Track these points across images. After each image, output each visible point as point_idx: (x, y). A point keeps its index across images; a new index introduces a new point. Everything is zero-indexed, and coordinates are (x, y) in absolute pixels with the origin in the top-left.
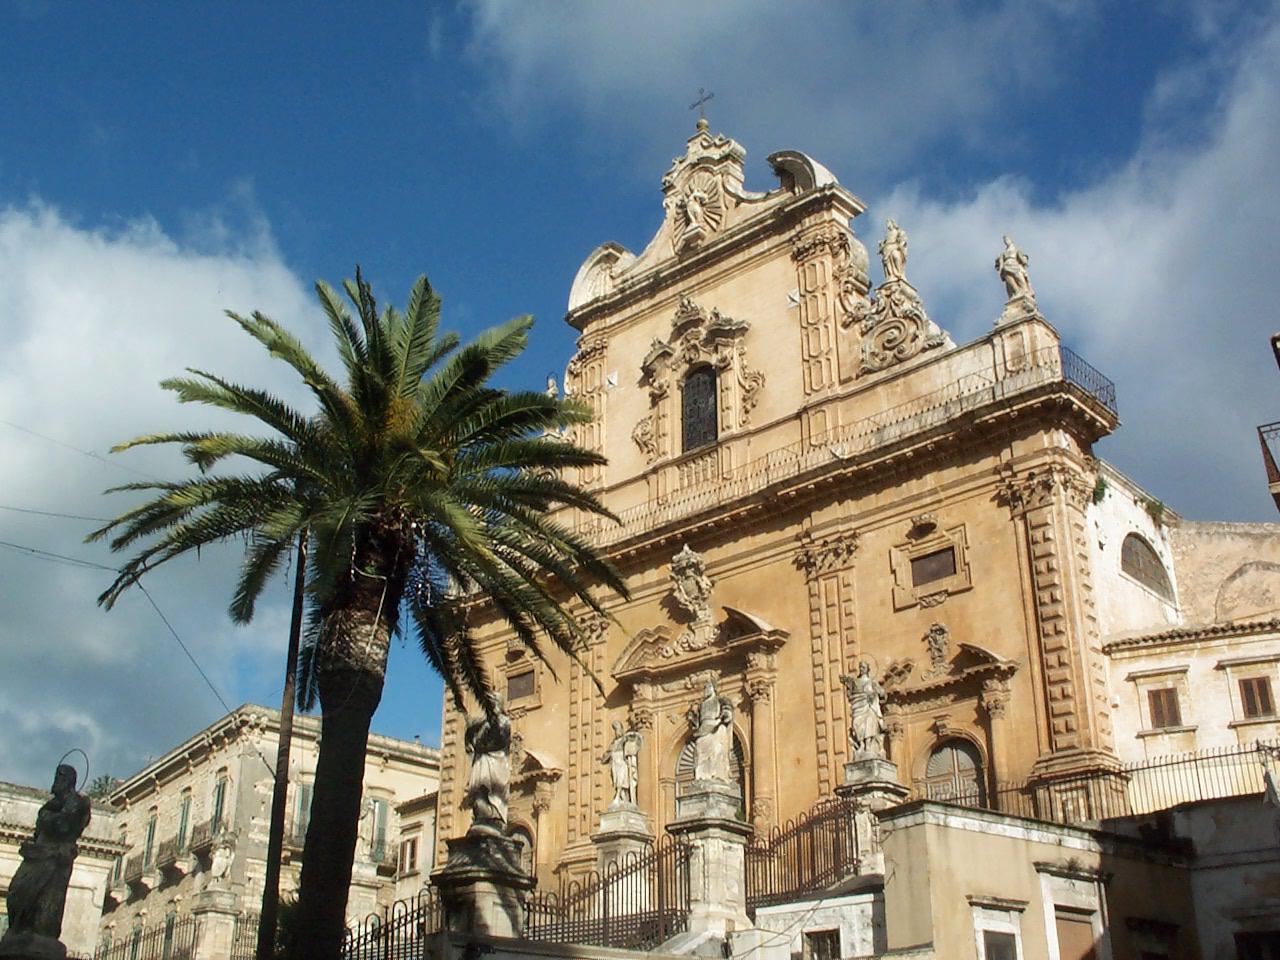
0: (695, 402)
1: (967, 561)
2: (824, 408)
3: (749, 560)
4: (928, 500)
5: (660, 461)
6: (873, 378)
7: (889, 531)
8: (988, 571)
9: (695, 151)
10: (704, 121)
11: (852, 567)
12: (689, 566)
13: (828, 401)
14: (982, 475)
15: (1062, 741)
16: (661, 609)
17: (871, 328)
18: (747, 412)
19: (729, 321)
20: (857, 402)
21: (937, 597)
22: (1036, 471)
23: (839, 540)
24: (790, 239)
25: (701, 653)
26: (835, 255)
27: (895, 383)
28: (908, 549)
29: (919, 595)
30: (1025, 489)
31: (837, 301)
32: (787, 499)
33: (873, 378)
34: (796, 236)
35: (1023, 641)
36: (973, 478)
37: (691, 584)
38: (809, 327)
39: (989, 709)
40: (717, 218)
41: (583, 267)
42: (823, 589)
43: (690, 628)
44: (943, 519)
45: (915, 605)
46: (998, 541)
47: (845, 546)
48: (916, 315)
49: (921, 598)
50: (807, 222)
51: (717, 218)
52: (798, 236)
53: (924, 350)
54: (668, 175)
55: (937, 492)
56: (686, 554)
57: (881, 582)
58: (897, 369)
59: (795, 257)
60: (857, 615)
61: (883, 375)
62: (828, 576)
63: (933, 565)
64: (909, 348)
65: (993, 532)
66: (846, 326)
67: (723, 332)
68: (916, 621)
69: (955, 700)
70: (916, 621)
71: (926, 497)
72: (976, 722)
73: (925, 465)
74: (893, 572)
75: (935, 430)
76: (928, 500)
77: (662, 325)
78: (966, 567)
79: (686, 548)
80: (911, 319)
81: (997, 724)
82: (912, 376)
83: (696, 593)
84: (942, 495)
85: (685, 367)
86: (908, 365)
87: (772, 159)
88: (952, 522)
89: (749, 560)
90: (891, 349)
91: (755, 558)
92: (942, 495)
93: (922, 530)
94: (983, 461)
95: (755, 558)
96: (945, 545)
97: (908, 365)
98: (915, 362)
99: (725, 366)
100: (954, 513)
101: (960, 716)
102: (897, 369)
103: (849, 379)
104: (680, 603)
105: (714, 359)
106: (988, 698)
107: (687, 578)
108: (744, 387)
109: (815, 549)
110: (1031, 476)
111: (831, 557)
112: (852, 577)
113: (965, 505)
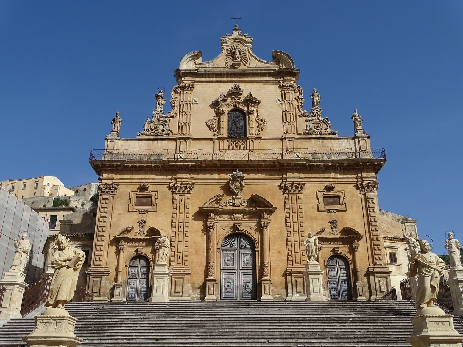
0: (234, 121)
1: (345, 202)
2: (293, 140)
3: (260, 181)
4: (332, 180)
5: (220, 136)
6: (310, 136)
7: (316, 186)
8: (352, 207)
9: (236, 34)
10: (237, 25)
11: (302, 194)
12: (239, 177)
13: (295, 138)
14: (351, 178)
15: (378, 263)
16: (221, 190)
17: (310, 121)
18: (259, 131)
19: (255, 99)
20: (304, 142)
21: (334, 211)
22: (371, 182)
23: (299, 184)
24: (279, 81)
25: (237, 208)
26: (295, 92)
27: (319, 140)
28: (323, 193)
29: (327, 209)
30: (366, 186)
31: (297, 107)
32: (283, 165)
33: (310, 136)
34: (283, 80)
35: (363, 230)
36: (348, 178)
37: (238, 183)
38: (285, 111)
40: (246, 61)
41: (186, 55)
42: (290, 198)
43: (233, 198)
44: (338, 187)
45: (325, 211)
46: (355, 199)
47: (300, 187)
48: (327, 122)
49: (328, 210)
50: (286, 78)
51: (246, 61)
52: (283, 81)
53: (329, 134)
54: (224, 38)
55: (335, 179)
56: (238, 173)
57: (312, 201)
58: (318, 136)
59: (280, 87)
60: (303, 209)
61: (314, 136)
62: (292, 194)
63: (331, 200)
64: (324, 132)
65: (353, 196)
66: (300, 116)
67: (251, 101)
68: (327, 217)
70: (327, 217)
71: (331, 179)
73: (331, 169)
74: (318, 199)
75: (342, 160)
76: (332, 180)
77: (226, 88)
78: (345, 204)
79: (238, 170)
80: (325, 123)
81: (357, 254)
82: (325, 140)
83: (239, 186)
84: (337, 180)
85: (232, 107)
86: (323, 136)
87: (275, 52)
88: (339, 189)
89: (260, 181)
90: (317, 129)
91: (262, 181)
92: (337, 180)
93: (329, 189)
94: (352, 175)
95: (262, 181)
96: (336, 195)
97: (323, 136)
98: (327, 136)
99: (250, 113)
100: (340, 186)
101: (343, 249)
102: (318, 136)
103: (301, 134)
104: (232, 188)
105: (246, 109)
107: (237, 181)
108: (258, 123)
109: (289, 184)
110: (369, 183)
111: (294, 188)
112: (301, 196)
113: (344, 185)
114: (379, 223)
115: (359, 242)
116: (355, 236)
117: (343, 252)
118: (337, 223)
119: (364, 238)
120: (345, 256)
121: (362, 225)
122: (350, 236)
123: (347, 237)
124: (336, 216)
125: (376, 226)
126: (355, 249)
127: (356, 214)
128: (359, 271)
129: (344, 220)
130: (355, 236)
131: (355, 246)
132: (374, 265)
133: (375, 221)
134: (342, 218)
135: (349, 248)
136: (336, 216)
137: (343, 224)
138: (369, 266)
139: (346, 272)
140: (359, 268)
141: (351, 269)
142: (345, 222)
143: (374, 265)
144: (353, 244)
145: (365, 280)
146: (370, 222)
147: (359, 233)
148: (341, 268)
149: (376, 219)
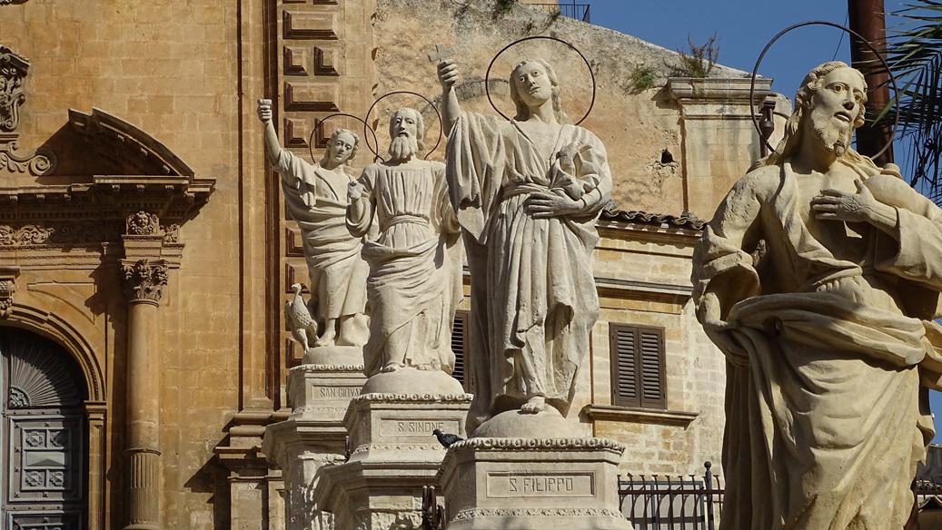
35: (226, 138)
39: (137, 279)
69: (52, 242)
72: (95, 304)
81: (147, 317)
106: (135, 253)
114: (353, 88)
115: (183, 233)
116: (141, 182)
117: (47, 305)
118: (29, 85)
119: (220, 209)
120: (61, 337)
121: (217, 98)
122: (100, 180)
123: (82, 188)
124: (28, 26)
125: (327, 107)
126: (137, 279)
127: (185, 13)
128: (155, 445)
129: (86, 63)
130: (141, 182)
131: (140, 263)
132: (277, 407)
133: (324, 70)
134: (68, 44)
135: (98, 275)
136: (28, 26)
137: (69, 92)
138: (241, 409)
139: (60, 458)
140: (150, 422)
141: (94, 435)
142: (88, 75)
143: (277, 407)
144: (127, 244)
145: (194, 518)
146: (282, 78)
147: (174, 160)
148: (25, 427)
149: (334, 57)
